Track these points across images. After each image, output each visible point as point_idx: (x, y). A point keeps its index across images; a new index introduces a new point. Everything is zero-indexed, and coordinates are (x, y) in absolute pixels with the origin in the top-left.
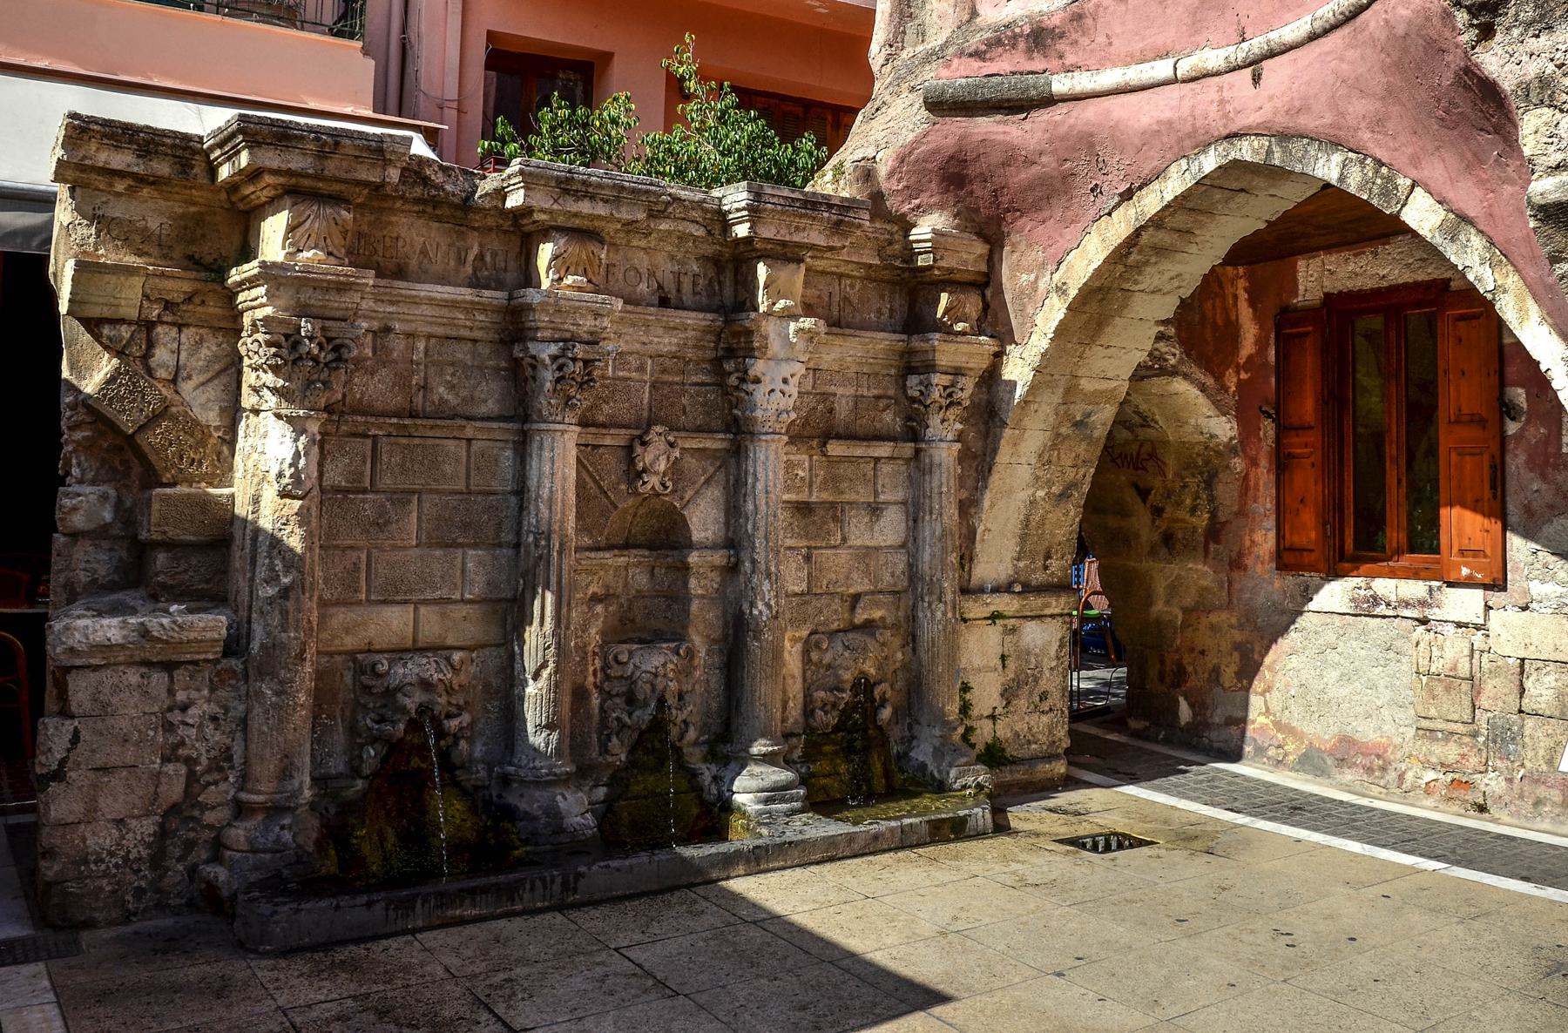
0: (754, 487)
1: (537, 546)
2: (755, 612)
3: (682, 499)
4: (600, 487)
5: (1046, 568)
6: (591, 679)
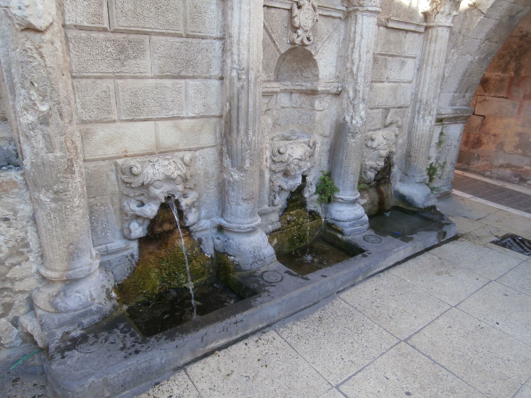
0: (360, 42)
1: (239, 79)
2: (354, 122)
3: (316, 48)
4: (271, 38)
5: (464, 96)
6: (264, 163)
